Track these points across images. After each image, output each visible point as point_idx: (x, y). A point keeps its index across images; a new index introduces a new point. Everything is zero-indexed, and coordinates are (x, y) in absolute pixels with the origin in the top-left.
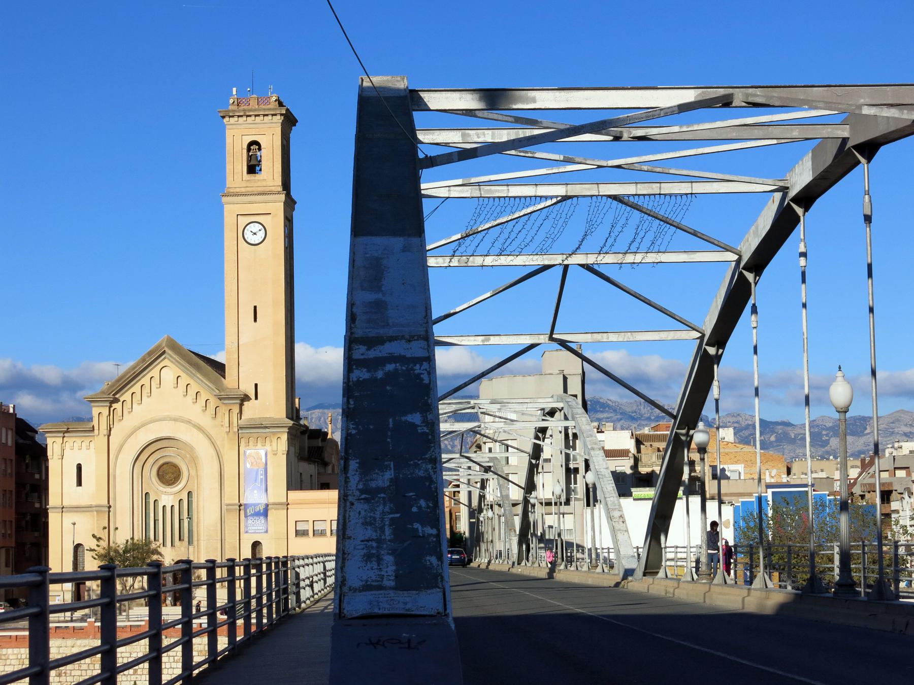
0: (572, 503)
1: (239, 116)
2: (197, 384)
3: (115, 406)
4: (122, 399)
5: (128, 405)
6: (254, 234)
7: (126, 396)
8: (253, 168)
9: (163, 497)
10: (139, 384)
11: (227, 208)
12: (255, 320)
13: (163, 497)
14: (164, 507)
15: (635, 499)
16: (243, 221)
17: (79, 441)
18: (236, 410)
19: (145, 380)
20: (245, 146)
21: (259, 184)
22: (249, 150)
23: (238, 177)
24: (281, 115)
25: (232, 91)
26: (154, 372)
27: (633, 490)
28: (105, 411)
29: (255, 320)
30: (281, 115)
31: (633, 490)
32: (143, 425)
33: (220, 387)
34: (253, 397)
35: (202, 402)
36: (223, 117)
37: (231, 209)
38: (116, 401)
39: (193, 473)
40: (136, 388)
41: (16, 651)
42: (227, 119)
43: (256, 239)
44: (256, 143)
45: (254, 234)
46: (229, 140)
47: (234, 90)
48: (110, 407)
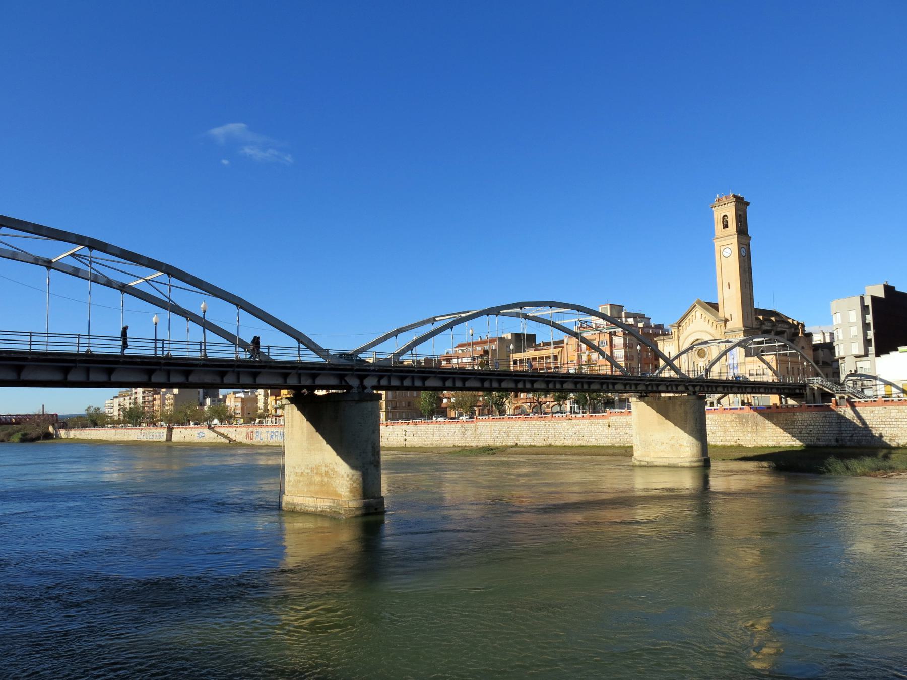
0: (869, 355)
1: (718, 206)
2: (709, 316)
3: (680, 328)
4: (682, 325)
5: (685, 327)
6: (727, 253)
7: (683, 324)
8: (726, 226)
9: (700, 363)
10: (688, 319)
11: (715, 244)
12: (729, 288)
13: (700, 363)
14: (700, 367)
15: (901, 352)
16: (722, 248)
17: (668, 343)
18: (723, 325)
19: (690, 317)
20: (722, 218)
21: (728, 232)
22: (723, 218)
23: (719, 231)
24: (734, 202)
25: (716, 196)
26: (693, 313)
27: (899, 347)
28: (676, 331)
29: (729, 288)
30: (734, 202)
31: (899, 347)
32: (690, 335)
33: (716, 316)
34: (730, 320)
35: (711, 323)
36: (712, 207)
37: (717, 244)
38: (680, 326)
39: (710, 353)
40: (687, 321)
41: (602, 420)
42: (714, 208)
43: (727, 255)
44: (726, 216)
45: (727, 253)
46: (715, 216)
47: (718, 195)
48: (678, 329)
